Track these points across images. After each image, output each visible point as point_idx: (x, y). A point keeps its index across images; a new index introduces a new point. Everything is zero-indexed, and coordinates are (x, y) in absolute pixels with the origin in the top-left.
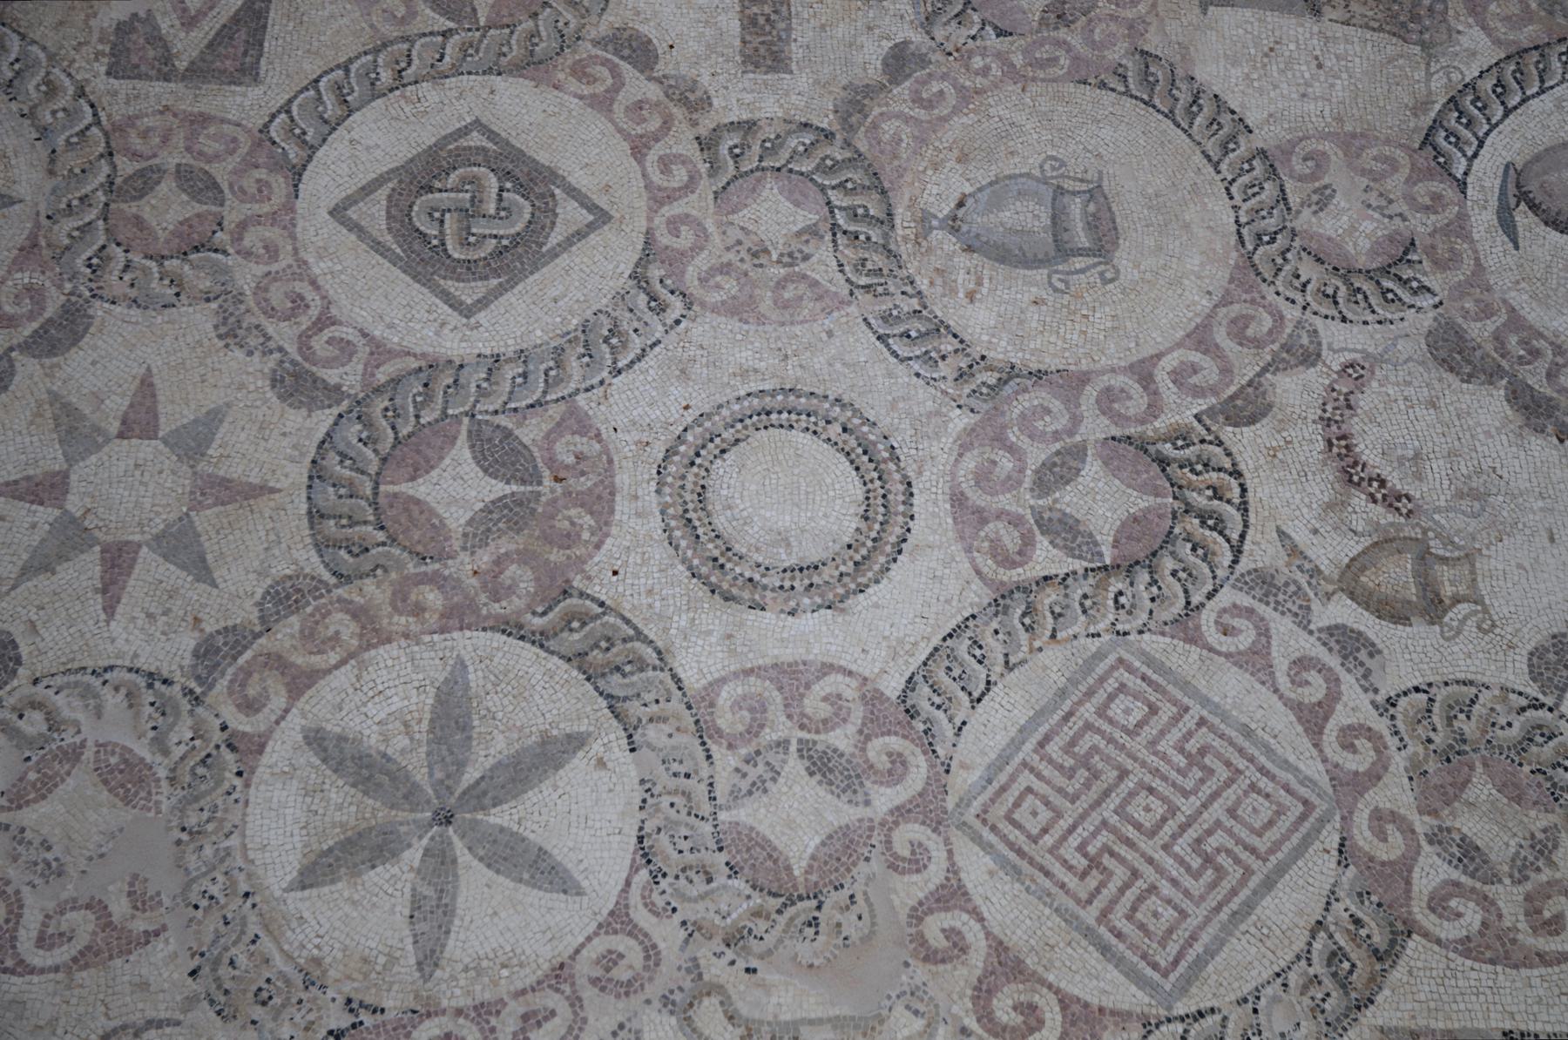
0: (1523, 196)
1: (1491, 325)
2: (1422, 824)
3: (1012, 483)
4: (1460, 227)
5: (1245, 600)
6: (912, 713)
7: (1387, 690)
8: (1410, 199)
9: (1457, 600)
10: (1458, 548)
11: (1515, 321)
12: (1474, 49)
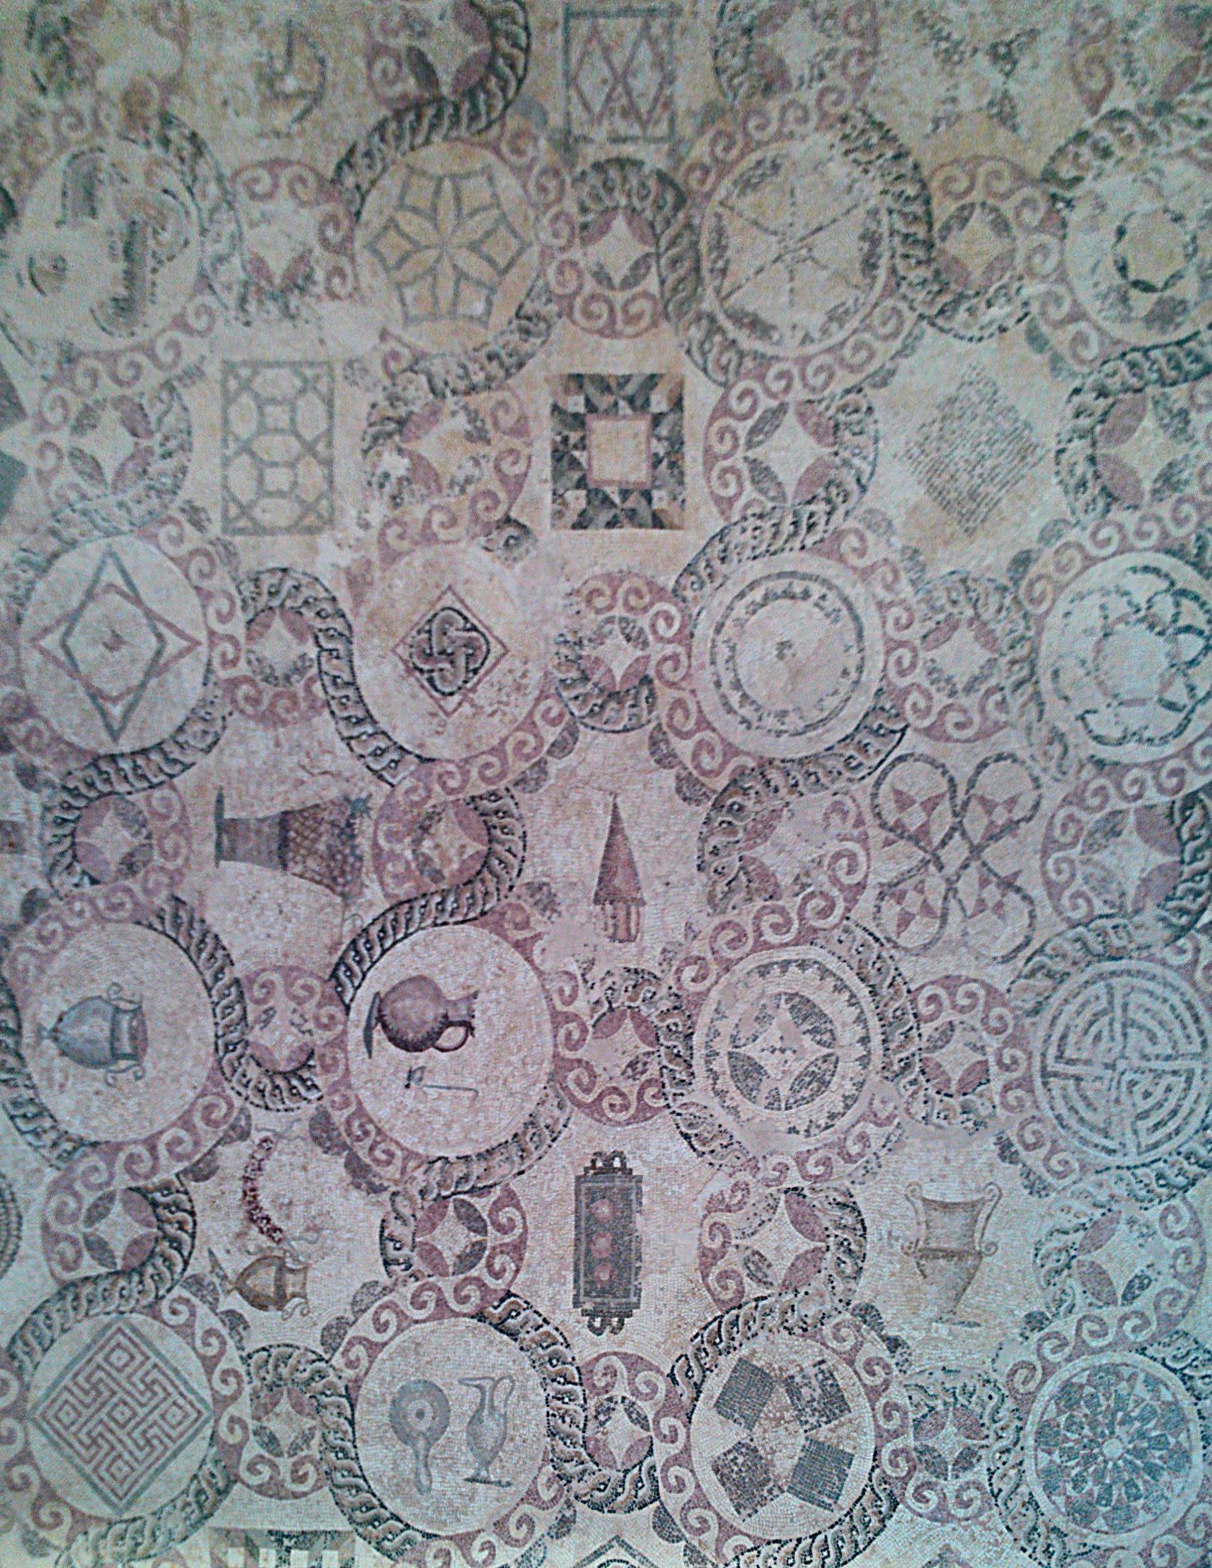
0: (381, 1019)
1: (347, 1112)
2: (252, 1425)
3: (74, 1217)
4: (340, 1042)
5: (186, 1294)
6: (13, 1357)
7: (249, 1350)
8: (317, 1019)
11: (360, 1111)
12: (374, 898)
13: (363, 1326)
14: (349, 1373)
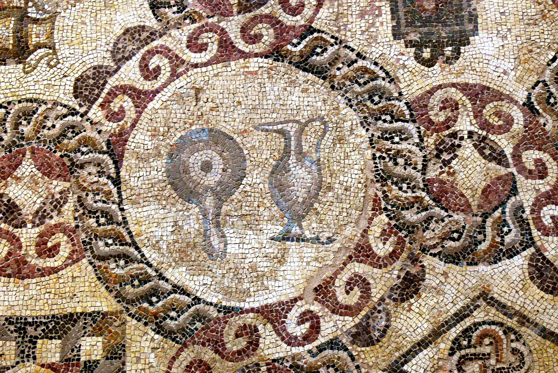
9: (38, 46)
10: (45, 12)
13: (130, 73)
14: (111, 127)
